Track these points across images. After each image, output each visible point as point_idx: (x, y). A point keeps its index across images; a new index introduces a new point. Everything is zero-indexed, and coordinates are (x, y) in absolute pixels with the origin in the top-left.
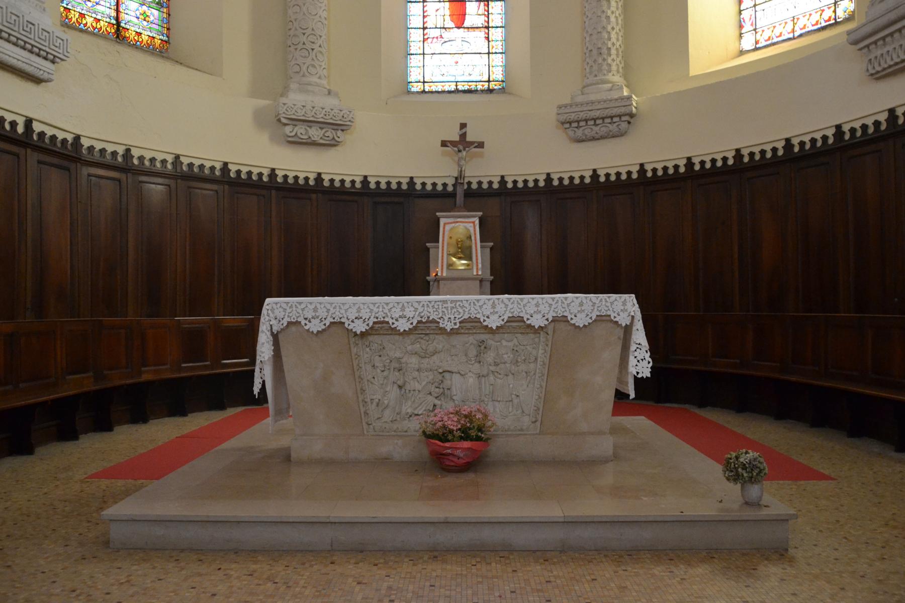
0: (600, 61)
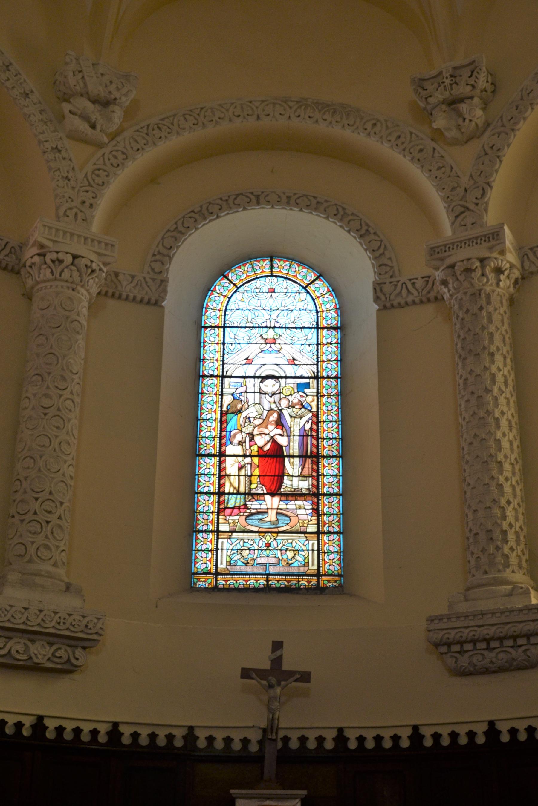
0: (492, 550)
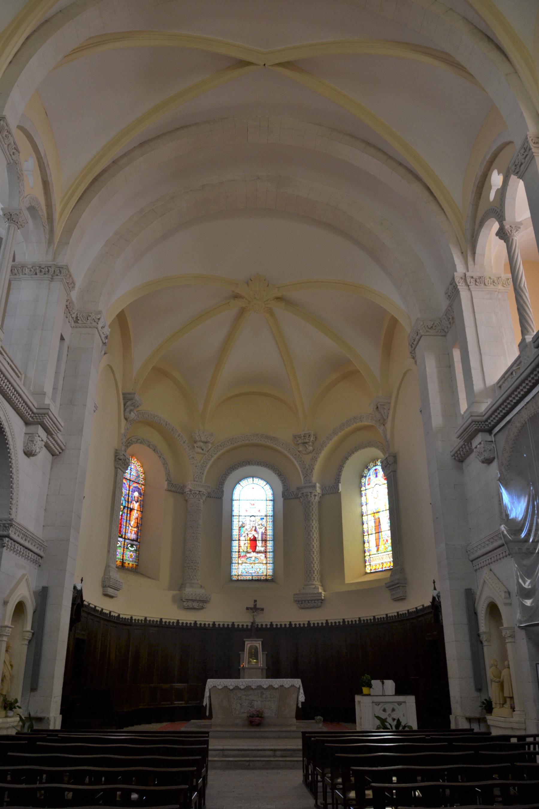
0: (310, 575)
